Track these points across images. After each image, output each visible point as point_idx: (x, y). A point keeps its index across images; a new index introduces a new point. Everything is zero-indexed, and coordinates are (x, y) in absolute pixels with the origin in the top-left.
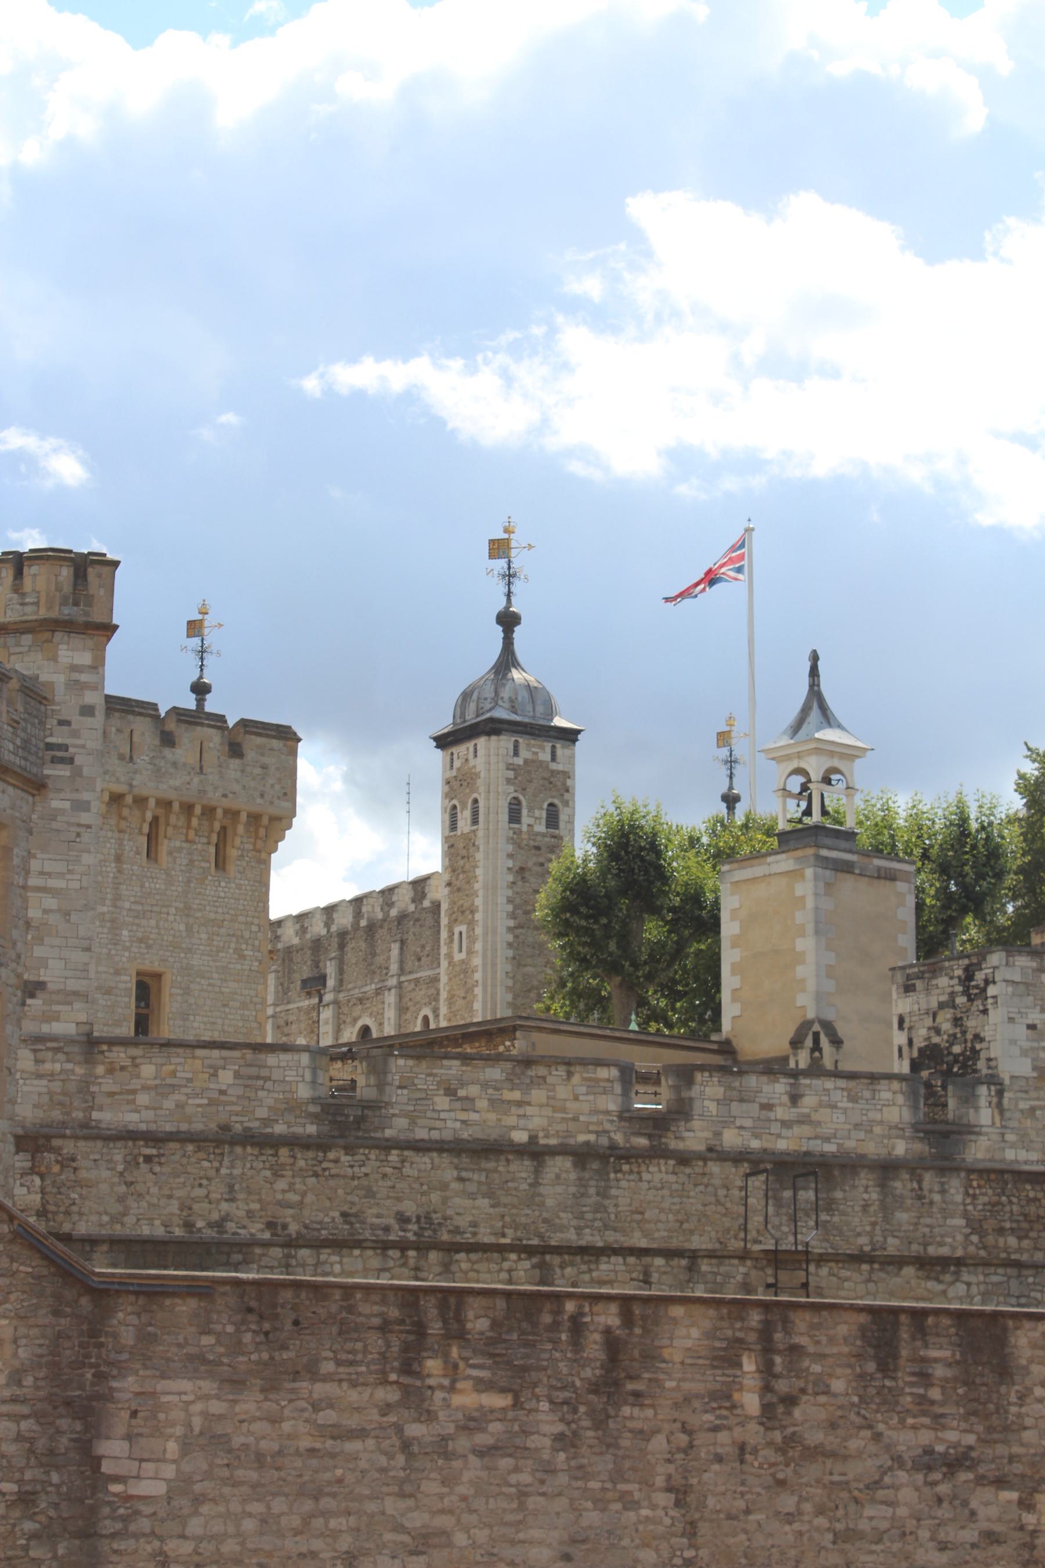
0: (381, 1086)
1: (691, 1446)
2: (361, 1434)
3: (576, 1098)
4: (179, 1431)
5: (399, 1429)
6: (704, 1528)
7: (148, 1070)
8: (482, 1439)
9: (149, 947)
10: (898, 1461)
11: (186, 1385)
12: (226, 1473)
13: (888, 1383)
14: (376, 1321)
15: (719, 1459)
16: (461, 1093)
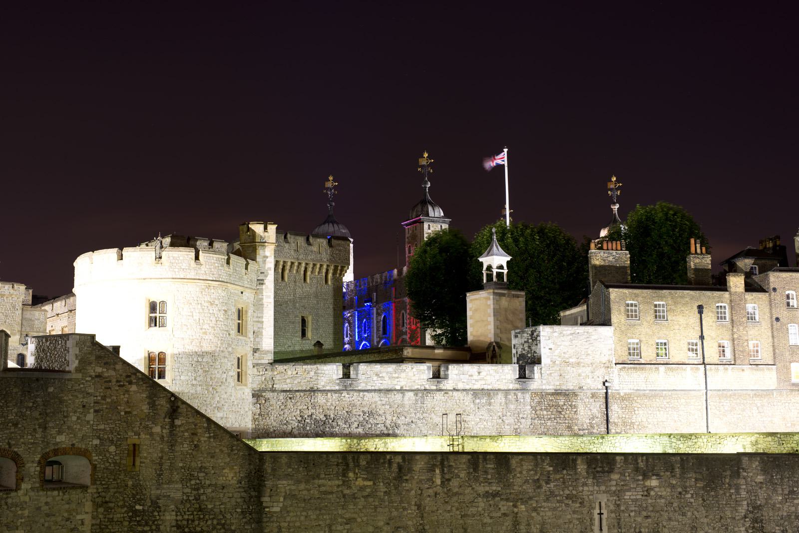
0: (357, 374)
1: (422, 493)
2: (332, 493)
3: (414, 375)
4: (283, 494)
5: (342, 492)
6: (425, 515)
7: (289, 373)
8: (366, 494)
9: (305, 308)
10: (479, 495)
11: (285, 482)
12: (296, 505)
13: (476, 474)
14: (336, 463)
15: (429, 496)
16: (380, 375)
